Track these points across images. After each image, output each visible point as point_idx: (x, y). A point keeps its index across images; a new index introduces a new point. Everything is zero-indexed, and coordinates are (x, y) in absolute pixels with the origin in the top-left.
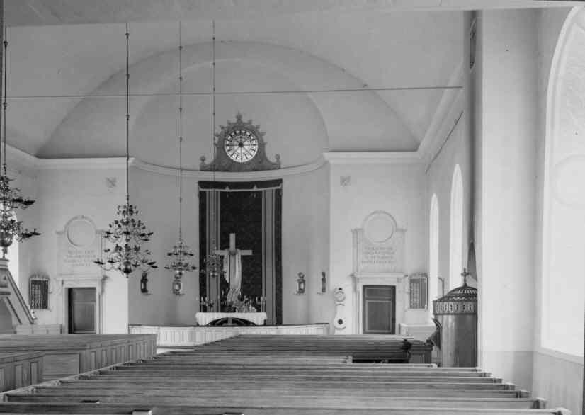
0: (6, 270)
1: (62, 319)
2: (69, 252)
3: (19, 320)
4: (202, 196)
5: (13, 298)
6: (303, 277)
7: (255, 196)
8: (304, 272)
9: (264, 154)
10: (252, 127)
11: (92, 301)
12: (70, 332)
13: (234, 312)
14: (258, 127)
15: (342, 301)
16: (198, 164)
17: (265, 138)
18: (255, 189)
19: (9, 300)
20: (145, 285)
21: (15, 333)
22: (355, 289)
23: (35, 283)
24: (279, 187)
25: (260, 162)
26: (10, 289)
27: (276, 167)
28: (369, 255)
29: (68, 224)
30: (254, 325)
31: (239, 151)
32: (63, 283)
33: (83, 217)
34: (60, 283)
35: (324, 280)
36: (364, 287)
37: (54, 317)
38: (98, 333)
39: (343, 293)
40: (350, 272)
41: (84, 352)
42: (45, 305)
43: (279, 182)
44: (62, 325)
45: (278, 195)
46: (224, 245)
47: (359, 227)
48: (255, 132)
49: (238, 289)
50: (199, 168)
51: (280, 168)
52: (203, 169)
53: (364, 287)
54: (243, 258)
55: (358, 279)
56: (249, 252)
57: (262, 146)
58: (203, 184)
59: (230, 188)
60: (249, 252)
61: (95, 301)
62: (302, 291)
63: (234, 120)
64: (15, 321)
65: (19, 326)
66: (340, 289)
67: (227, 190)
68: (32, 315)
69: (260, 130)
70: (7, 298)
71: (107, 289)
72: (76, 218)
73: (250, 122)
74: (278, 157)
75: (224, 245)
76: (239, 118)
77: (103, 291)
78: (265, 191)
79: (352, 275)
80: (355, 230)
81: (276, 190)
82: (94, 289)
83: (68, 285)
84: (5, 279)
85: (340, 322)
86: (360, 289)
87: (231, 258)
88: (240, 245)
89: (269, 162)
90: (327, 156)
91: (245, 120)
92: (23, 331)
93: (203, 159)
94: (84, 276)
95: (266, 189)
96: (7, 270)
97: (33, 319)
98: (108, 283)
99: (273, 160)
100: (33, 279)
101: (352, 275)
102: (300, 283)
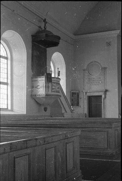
0: (59, 84)
1: (86, 111)
2: (89, 79)
3: (66, 111)
5: (62, 99)
11: (100, 102)
12: (89, 117)
19: (60, 100)
21: (64, 116)
23: (73, 94)
26: (61, 94)
29: (88, 65)
32: (86, 94)
33: (95, 62)
34: (85, 94)
37: (83, 108)
38: (103, 117)
41: (110, 130)
42: (78, 104)
44: (86, 114)
61: (102, 102)
64: (63, 111)
65: (65, 113)
68: (72, 109)
70: (60, 99)
71: (107, 96)
72: (92, 62)
77: (105, 97)
82: (101, 96)
83: (89, 94)
84: (58, 88)
92: (68, 115)
94: (95, 89)
96: (60, 84)
97: (72, 110)
98: (107, 93)
100: (72, 92)
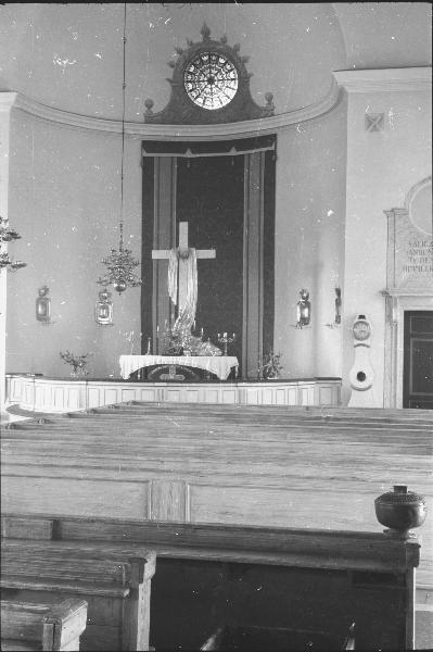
4: (147, 166)
6: (307, 297)
7: (233, 163)
8: (309, 288)
9: (249, 92)
10: (228, 48)
13: (181, 354)
14: (237, 48)
15: (362, 339)
16: (140, 114)
17: (249, 67)
18: (233, 152)
20: (45, 305)
22: (389, 317)
24: (273, 148)
25: (242, 107)
27: (268, 113)
28: (417, 257)
30: (214, 379)
31: (208, 90)
35: (338, 303)
36: (407, 314)
39: (367, 324)
40: (383, 287)
43: (270, 139)
45: (270, 161)
46: (173, 243)
47: (399, 205)
48: (236, 59)
49: (192, 314)
50: (143, 119)
51: (273, 115)
52: (150, 119)
53: (407, 314)
54: (202, 265)
55: (396, 299)
56: (210, 254)
57: (244, 81)
58: (148, 145)
59: (193, 153)
60: (210, 254)
62: (304, 321)
63: (199, 39)
66: (362, 317)
67: (189, 154)
69: (241, 54)
73: (224, 41)
74: (270, 98)
75: (173, 243)
76: (206, 33)
78: (249, 155)
79: (385, 294)
80: (392, 210)
81: (267, 152)
85: (361, 376)
86: (399, 317)
87: (181, 261)
88: (195, 242)
89: (257, 107)
90: (342, 78)
91: (214, 37)
93: (149, 105)
95: (249, 152)
99: (263, 103)
101: (385, 294)
102: (302, 308)
